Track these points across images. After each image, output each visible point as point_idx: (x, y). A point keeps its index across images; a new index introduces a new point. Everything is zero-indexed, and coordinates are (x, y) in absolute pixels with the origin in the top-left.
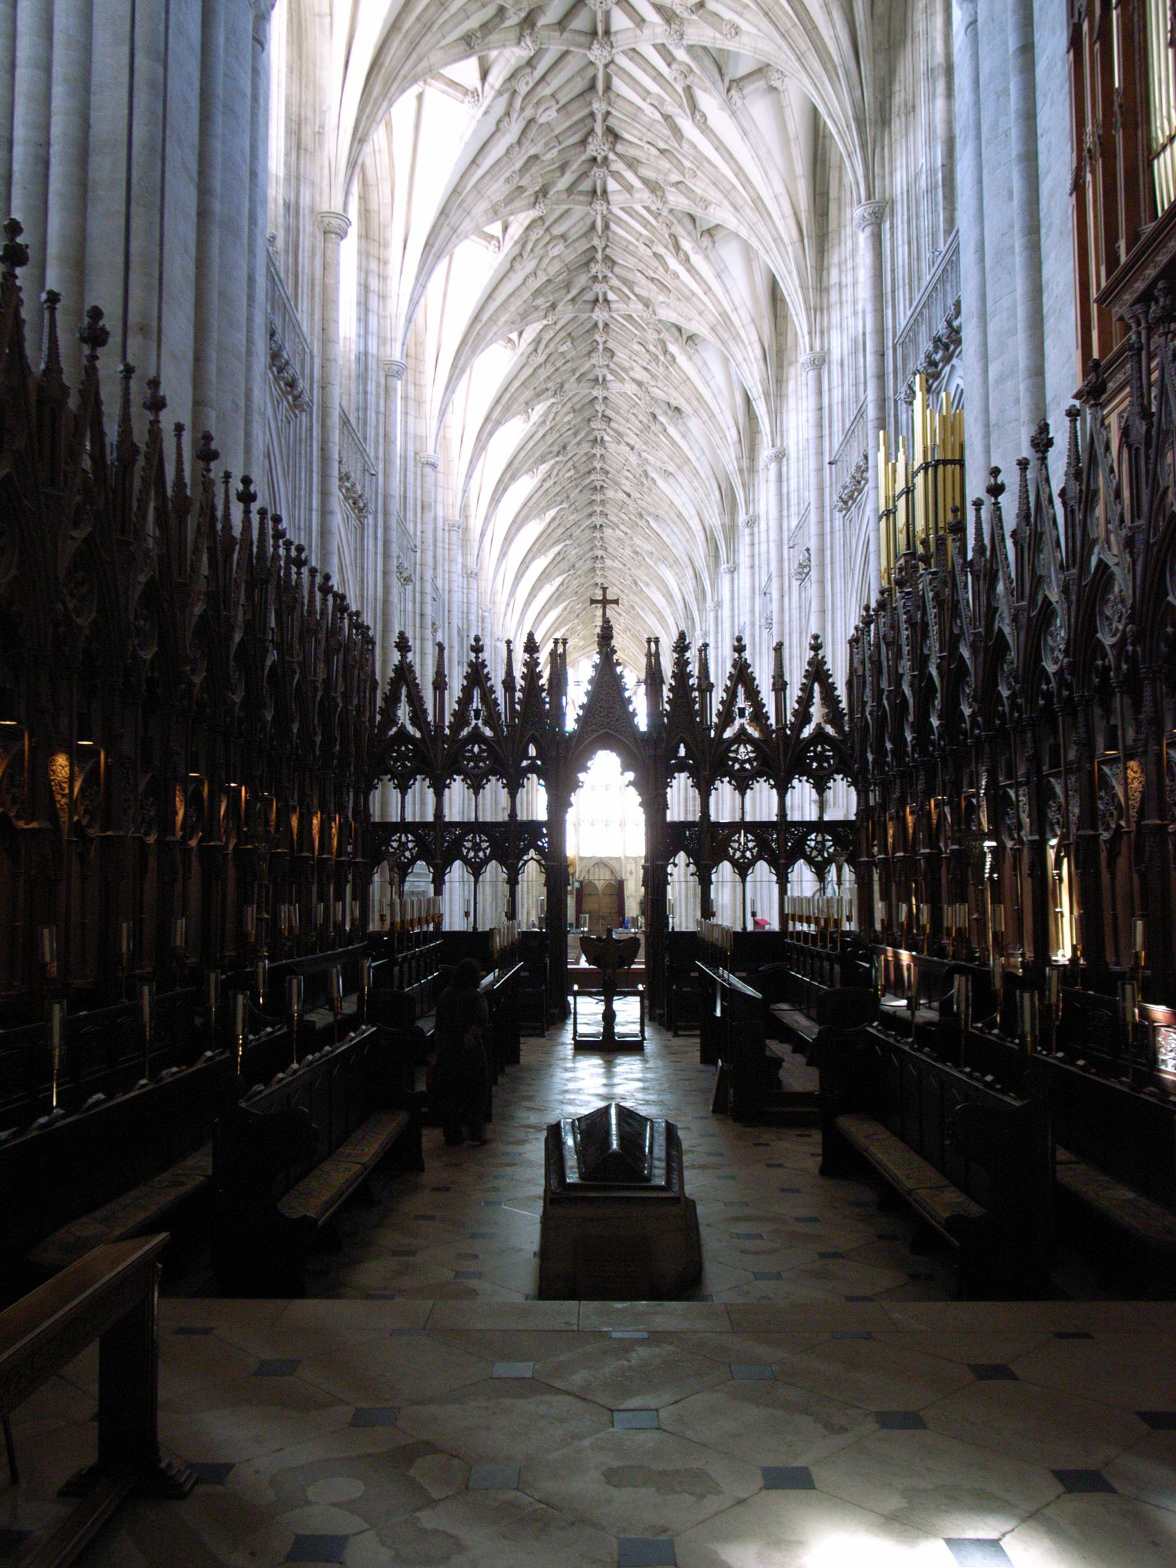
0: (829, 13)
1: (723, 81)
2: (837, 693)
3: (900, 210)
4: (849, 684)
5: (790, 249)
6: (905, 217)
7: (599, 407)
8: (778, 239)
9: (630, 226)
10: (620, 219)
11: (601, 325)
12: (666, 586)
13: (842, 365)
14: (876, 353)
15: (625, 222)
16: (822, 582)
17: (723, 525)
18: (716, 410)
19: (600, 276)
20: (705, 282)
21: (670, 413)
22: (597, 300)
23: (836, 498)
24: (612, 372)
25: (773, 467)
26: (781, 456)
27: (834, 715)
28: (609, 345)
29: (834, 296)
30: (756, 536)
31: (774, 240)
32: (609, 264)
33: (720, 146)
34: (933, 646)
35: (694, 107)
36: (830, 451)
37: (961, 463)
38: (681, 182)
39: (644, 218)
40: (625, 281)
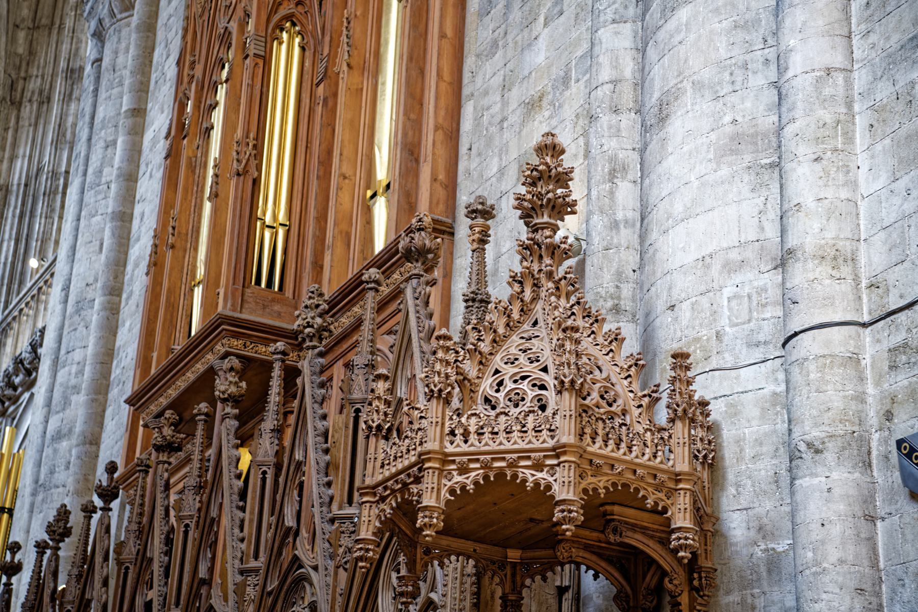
6: (18, 211)
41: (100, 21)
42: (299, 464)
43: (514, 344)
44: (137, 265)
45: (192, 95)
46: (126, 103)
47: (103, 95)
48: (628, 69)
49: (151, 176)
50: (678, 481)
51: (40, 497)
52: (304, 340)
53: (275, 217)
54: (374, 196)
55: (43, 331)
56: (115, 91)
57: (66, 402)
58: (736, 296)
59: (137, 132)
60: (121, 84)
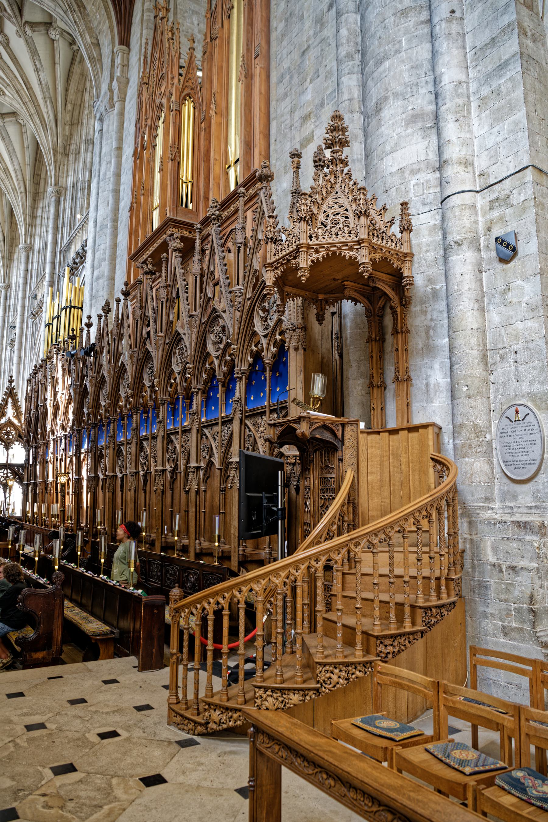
0: (46, 102)
2: (19, 403)
3: (69, 193)
8: (14, 189)
13: (39, 253)
14: (52, 252)
16: (20, 350)
23: (30, 312)
27: (18, 416)
29: (38, 221)
37: (82, 309)
41: (101, 114)
42: (212, 272)
43: (330, 201)
44: (123, 209)
45: (147, 132)
46: (114, 145)
47: (104, 143)
48: (356, 93)
50: (405, 257)
51: (94, 301)
52: (211, 221)
53: (187, 178)
54: (229, 167)
55: (86, 241)
56: (109, 141)
57: (100, 265)
58: (417, 184)
59: (119, 156)
60: (111, 138)
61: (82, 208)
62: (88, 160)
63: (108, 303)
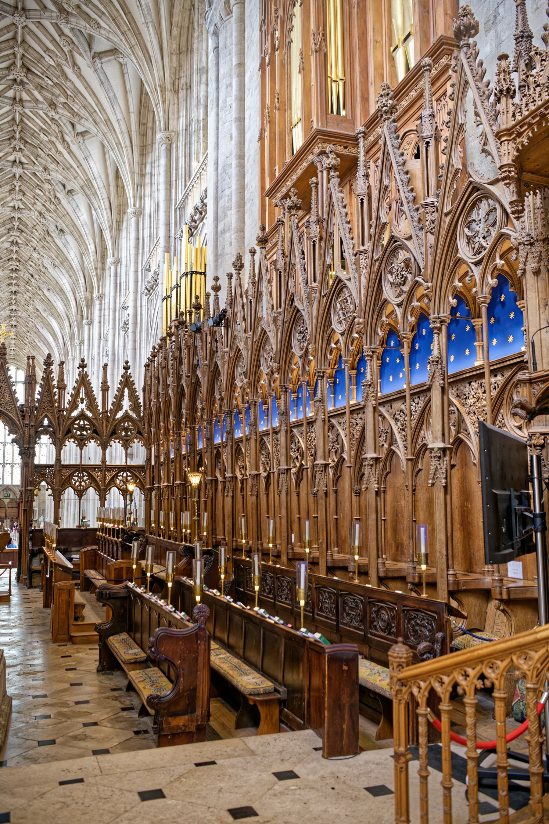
0: (148, 27)
1: (90, 51)
4: (144, 389)
5: (124, 150)
7: (16, 224)
9: (35, 122)
10: (30, 117)
11: (17, 176)
12: (53, 330)
15: (33, 119)
16: (135, 333)
17: (86, 298)
18: (83, 233)
19: (18, 148)
20: (78, 161)
21: (57, 232)
22: (15, 161)
24: (24, 204)
25: (113, 268)
26: (117, 262)
28: (24, 188)
30: (103, 305)
31: (116, 144)
32: (23, 141)
33: (88, 87)
34: (184, 370)
35: (75, 64)
36: (142, 262)
38: (66, 103)
39: (44, 120)
40: (32, 153)
44: (250, 141)
45: (279, 27)
46: (235, 61)
47: (221, 62)
49: (252, 95)
55: (206, 191)
56: (228, 58)
59: (241, 75)
60: (230, 54)
61: (198, 154)
62: (202, 94)
63: (240, 258)
